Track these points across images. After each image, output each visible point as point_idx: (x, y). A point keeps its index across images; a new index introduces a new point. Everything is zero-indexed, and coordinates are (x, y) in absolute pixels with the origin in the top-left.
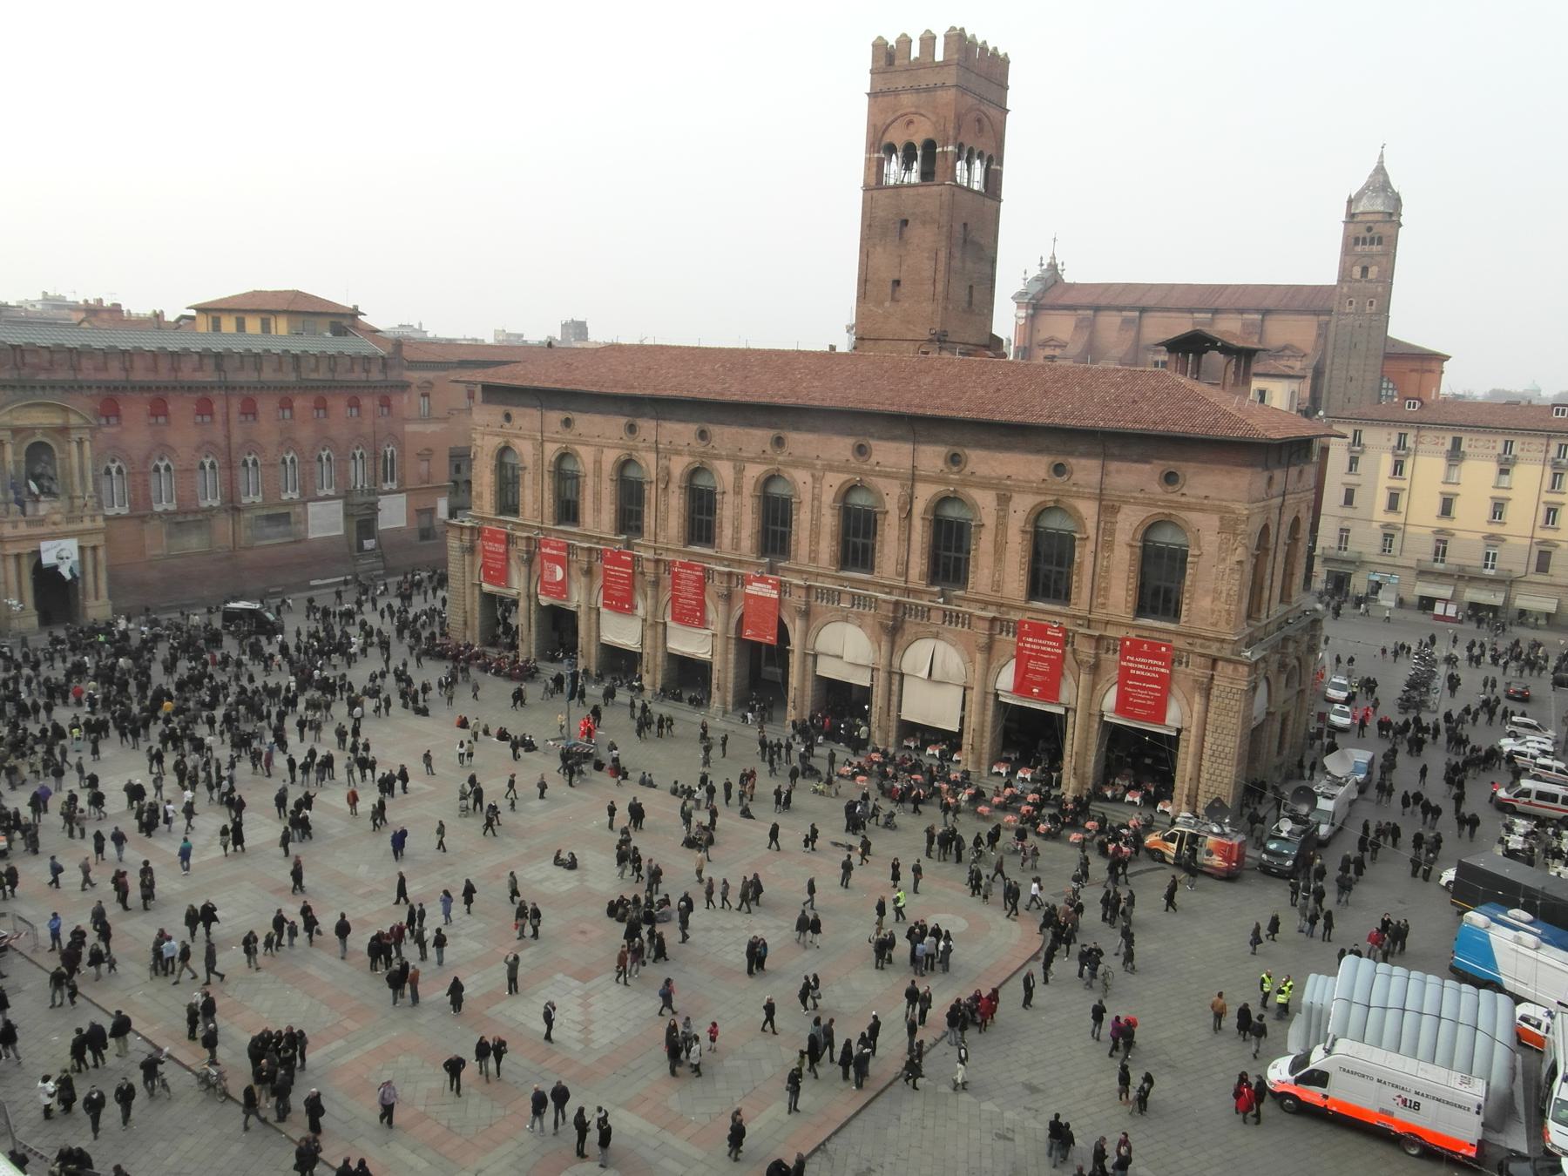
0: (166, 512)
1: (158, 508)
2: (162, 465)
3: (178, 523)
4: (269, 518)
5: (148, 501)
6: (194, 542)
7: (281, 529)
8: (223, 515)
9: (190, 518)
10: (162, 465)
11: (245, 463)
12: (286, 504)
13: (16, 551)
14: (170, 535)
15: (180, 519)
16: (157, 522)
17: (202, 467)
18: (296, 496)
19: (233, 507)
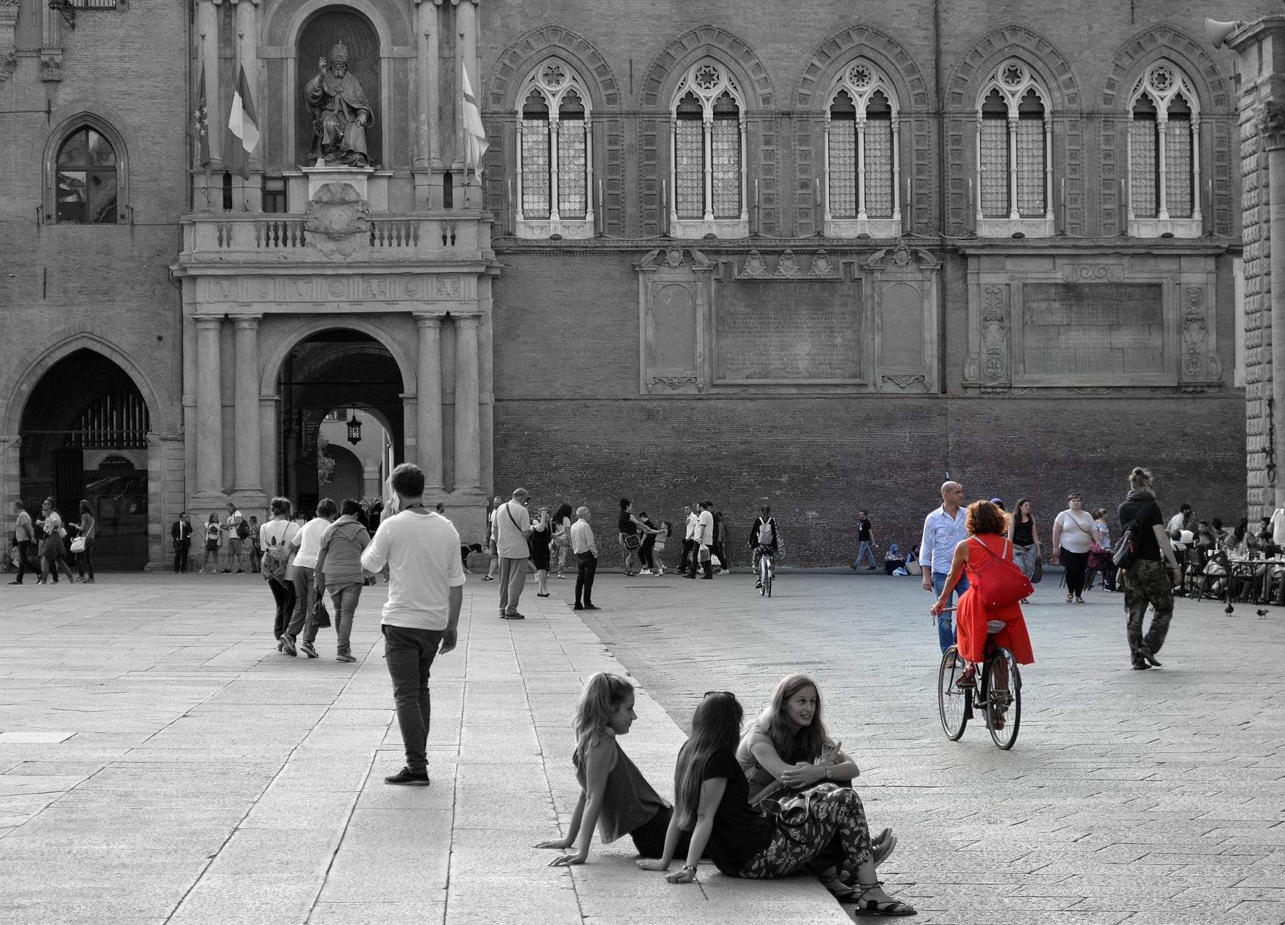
0: (712, 247)
1: (684, 230)
2: (708, 97)
3: (750, 283)
4: (1071, 292)
5: (654, 202)
6: (798, 352)
7: (1124, 338)
8: (911, 274)
9: (788, 269)
10: (708, 97)
11: (996, 110)
12: (1148, 251)
13: (220, 310)
14: (721, 322)
15: (755, 268)
16: (682, 275)
17: (844, 112)
18: (1188, 230)
19: (947, 248)
